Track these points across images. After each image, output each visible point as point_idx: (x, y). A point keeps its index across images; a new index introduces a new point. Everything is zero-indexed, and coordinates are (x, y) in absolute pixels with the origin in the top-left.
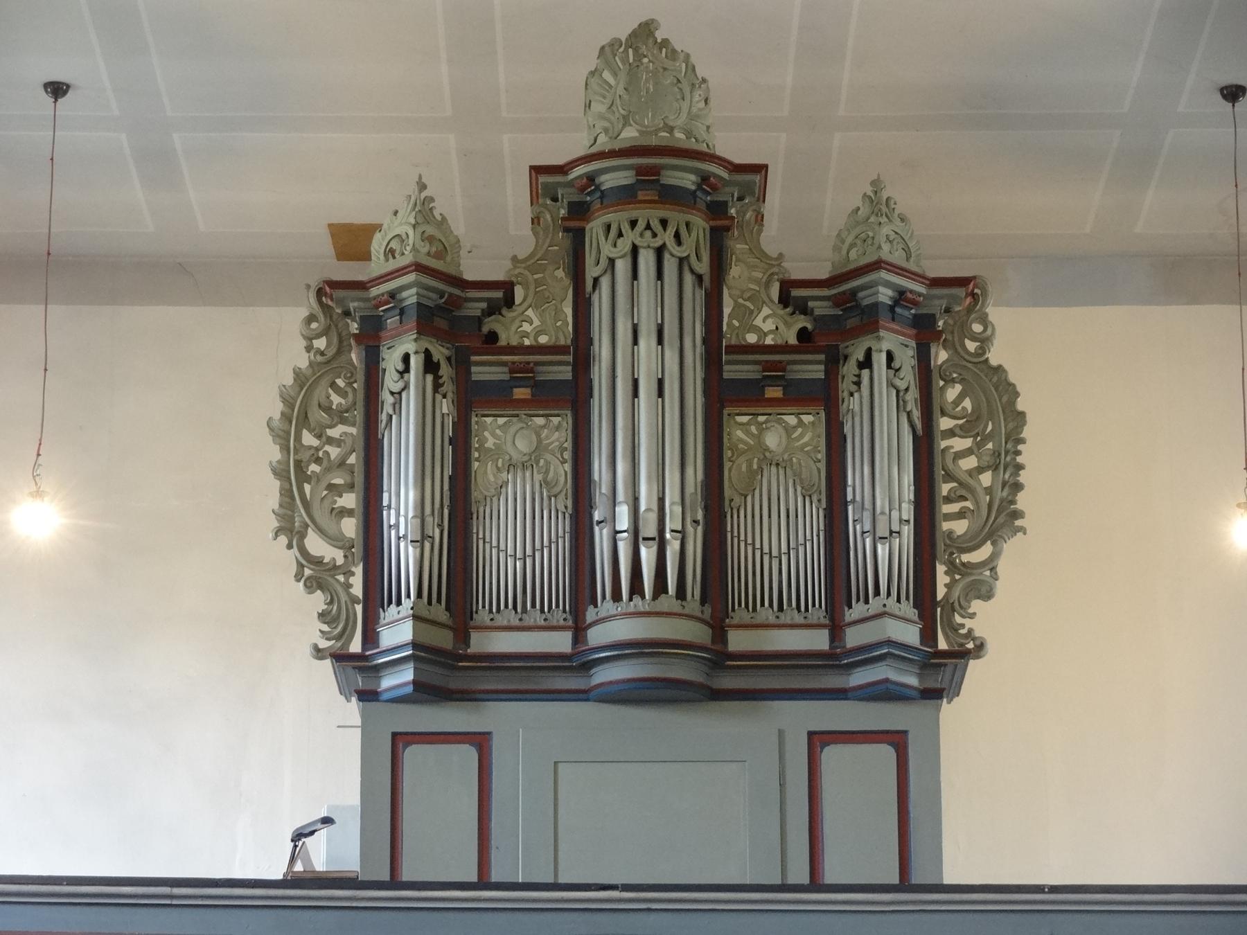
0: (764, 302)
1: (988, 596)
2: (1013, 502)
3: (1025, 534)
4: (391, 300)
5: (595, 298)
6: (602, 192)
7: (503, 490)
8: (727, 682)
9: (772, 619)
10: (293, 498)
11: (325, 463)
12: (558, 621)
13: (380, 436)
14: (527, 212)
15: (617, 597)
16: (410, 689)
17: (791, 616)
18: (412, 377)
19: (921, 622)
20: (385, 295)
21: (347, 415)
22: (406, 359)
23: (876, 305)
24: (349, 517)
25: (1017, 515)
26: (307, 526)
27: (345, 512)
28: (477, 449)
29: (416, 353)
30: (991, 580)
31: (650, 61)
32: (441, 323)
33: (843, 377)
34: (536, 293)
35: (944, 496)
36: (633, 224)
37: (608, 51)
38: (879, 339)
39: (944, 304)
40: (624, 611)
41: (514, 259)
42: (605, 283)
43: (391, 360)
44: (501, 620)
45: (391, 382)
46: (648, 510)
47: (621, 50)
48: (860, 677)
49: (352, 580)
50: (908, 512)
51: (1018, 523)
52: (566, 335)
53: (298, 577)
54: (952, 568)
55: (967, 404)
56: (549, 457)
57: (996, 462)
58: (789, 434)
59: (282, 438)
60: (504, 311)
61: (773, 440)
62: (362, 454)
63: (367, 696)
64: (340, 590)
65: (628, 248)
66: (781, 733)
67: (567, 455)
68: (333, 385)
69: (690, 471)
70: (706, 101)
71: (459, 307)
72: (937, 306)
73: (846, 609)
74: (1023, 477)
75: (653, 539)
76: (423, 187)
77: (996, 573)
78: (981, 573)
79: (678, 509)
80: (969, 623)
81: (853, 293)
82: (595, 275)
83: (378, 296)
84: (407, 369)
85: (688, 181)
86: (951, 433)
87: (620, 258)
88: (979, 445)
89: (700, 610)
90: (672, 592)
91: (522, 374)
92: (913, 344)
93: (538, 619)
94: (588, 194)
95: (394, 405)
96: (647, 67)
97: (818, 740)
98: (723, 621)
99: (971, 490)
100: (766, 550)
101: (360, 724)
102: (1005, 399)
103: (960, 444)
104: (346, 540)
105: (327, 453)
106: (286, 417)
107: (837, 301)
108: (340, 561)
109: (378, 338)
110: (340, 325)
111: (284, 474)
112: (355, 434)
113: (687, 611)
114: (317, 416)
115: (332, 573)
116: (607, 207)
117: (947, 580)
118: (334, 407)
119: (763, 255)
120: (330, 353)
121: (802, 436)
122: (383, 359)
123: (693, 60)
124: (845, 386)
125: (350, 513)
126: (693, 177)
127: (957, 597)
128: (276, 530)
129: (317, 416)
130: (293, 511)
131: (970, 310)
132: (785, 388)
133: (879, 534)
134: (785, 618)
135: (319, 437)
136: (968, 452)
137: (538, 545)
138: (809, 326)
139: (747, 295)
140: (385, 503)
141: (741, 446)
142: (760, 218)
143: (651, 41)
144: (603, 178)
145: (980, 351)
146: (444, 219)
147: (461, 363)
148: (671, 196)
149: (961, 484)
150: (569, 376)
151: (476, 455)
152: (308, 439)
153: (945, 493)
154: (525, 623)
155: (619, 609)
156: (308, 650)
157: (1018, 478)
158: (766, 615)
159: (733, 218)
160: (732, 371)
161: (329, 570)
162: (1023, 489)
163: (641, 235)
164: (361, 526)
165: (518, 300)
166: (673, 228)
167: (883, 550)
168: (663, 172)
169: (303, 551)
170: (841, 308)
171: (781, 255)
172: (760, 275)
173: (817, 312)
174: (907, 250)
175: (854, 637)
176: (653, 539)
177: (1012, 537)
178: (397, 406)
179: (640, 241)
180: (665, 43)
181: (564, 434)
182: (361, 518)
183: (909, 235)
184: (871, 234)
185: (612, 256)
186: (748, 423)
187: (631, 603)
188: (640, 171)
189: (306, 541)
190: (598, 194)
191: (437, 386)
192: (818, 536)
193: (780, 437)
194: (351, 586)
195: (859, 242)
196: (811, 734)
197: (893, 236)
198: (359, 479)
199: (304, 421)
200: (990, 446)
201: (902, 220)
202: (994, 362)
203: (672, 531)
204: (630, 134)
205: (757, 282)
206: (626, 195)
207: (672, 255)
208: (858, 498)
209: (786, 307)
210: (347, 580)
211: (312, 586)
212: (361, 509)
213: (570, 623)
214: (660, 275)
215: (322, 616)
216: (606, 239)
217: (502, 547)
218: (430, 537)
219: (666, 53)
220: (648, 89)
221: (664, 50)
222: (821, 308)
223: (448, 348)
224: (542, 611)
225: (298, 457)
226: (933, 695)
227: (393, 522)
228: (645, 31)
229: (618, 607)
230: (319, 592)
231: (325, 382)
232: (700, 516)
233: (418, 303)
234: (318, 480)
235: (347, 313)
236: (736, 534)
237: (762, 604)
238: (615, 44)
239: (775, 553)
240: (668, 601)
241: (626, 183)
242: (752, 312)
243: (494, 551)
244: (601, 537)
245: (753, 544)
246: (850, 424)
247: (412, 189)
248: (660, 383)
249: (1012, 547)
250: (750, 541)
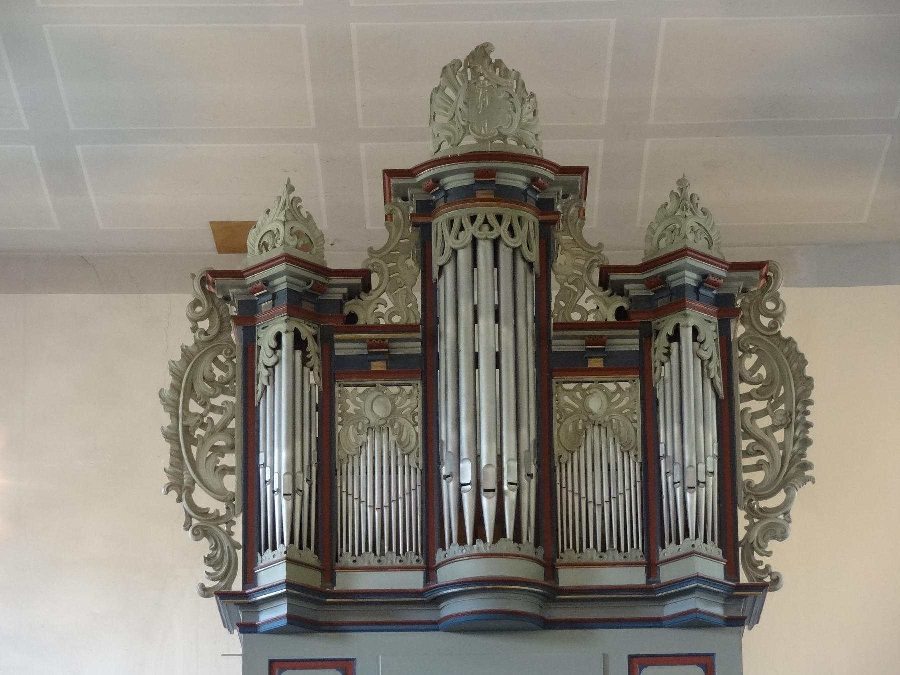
0: (586, 286)
1: (783, 537)
2: (803, 455)
3: (814, 483)
4: (265, 287)
5: (441, 283)
6: (446, 192)
7: (364, 450)
8: (559, 613)
9: (596, 559)
10: (182, 458)
11: (209, 428)
12: (412, 562)
13: (256, 404)
14: (382, 211)
15: (462, 541)
16: (284, 622)
17: (613, 556)
18: (284, 353)
19: (725, 560)
20: (260, 283)
21: (228, 386)
22: (278, 337)
23: (683, 288)
24: (231, 474)
25: (807, 466)
26: (194, 482)
27: (227, 470)
28: (340, 415)
29: (287, 332)
30: (785, 523)
31: (486, 79)
32: (307, 306)
33: (656, 349)
34: (390, 279)
35: (743, 451)
36: (473, 219)
37: (450, 71)
38: (686, 316)
39: (742, 285)
40: (468, 553)
41: (371, 251)
42: (449, 271)
43: (265, 339)
44: (362, 563)
45: (265, 357)
46: (488, 466)
47: (461, 70)
48: (673, 608)
49: (233, 529)
50: (713, 464)
51: (808, 473)
52: (416, 316)
53: (187, 526)
54: (752, 513)
55: (763, 371)
56: (402, 421)
57: (788, 421)
58: (609, 399)
59: (172, 406)
60: (363, 295)
61: (595, 404)
62: (241, 419)
63: (248, 629)
64: (223, 537)
65: (469, 239)
66: (605, 658)
67: (418, 419)
68: (216, 360)
69: (524, 432)
70: (535, 113)
71: (324, 292)
72: (735, 288)
73: (660, 549)
74: (812, 434)
75: (493, 491)
76: (291, 189)
77: (789, 517)
78: (777, 517)
79: (514, 465)
80: (766, 560)
81: (664, 277)
82: (441, 264)
83: (254, 284)
84: (279, 347)
85: (520, 182)
86: (749, 397)
87: (463, 248)
88: (774, 407)
89: (535, 552)
90: (510, 535)
91: (379, 350)
92: (716, 320)
93: (395, 561)
94: (434, 194)
95: (268, 377)
96: (484, 84)
98: (554, 561)
99: (767, 446)
100: (591, 499)
101: (241, 653)
102: (795, 366)
103: (757, 406)
104: (228, 494)
105: (210, 419)
106: (176, 389)
107: (650, 284)
108: (223, 512)
109: (254, 320)
110: (221, 309)
111: (174, 438)
112: (235, 402)
113: (523, 553)
114: (203, 387)
115: (216, 523)
116: (451, 205)
117: (747, 523)
118: (217, 379)
119: (585, 245)
120: (213, 333)
121: (620, 401)
122: (259, 338)
123: (524, 78)
124: (658, 357)
125: (231, 471)
126: (524, 179)
127: (756, 538)
128: (167, 486)
129: (203, 387)
131: (764, 290)
132: (605, 358)
133: (688, 484)
134: (608, 558)
135: (204, 405)
136: (764, 413)
137: (394, 498)
138: (626, 306)
139: (571, 280)
140: (262, 462)
141: (568, 410)
142: (582, 213)
143: (487, 61)
144: (447, 180)
145: (773, 326)
146: (310, 217)
147: (326, 340)
148: (506, 195)
149: (759, 441)
150: (419, 351)
151: (340, 419)
152: (195, 407)
153: (744, 448)
154: (384, 565)
155: (465, 551)
156: (196, 590)
157: (807, 435)
158: (591, 555)
159: (558, 213)
160: (559, 346)
161: (214, 520)
162: (812, 444)
163: (480, 229)
164: (241, 482)
165: (374, 286)
166: (507, 222)
167: (692, 498)
168: (498, 174)
169: (191, 504)
170: (654, 289)
171: (601, 245)
172: (582, 262)
173: (633, 294)
174: (710, 240)
175: (667, 574)
176: (493, 491)
177: (803, 486)
178: (271, 378)
179: (479, 234)
180: (499, 63)
181: (415, 401)
182: (241, 475)
183: (711, 226)
184: (678, 226)
185: (455, 247)
186: (574, 390)
187: (475, 546)
188: (479, 173)
189: (193, 495)
190: (443, 194)
191: (305, 361)
192: (636, 486)
193: (602, 401)
194: (232, 534)
195: (668, 233)
196: (631, 658)
197: (697, 228)
198: (239, 442)
199: (191, 391)
200: (783, 407)
201: (705, 214)
202: (785, 335)
203: (510, 484)
204: (469, 143)
205: (581, 269)
206: (467, 195)
207: (508, 246)
208: (670, 454)
209: (605, 289)
210: (229, 528)
211: (199, 535)
212: (241, 466)
213: (422, 564)
214: (496, 264)
215: (208, 560)
216: (450, 232)
217: (363, 499)
218: (301, 491)
219: (500, 73)
220: (484, 103)
221: (498, 70)
222: (635, 290)
223: (314, 328)
224: (398, 554)
225: (184, 424)
226: (736, 622)
227: (268, 478)
228: (482, 53)
229: (463, 550)
230: (205, 539)
231: (209, 357)
232: (533, 470)
233: (289, 290)
234: (203, 443)
235: (227, 299)
236: (564, 486)
237: (588, 546)
238: (456, 64)
239: (598, 501)
240: (507, 545)
241: (466, 184)
242: (576, 294)
243: (356, 503)
244: (449, 490)
245: (580, 494)
246: (662, 389)
247: (282, 191)
248: (498, 356)
249: (802, 494)
250: (576, 491)
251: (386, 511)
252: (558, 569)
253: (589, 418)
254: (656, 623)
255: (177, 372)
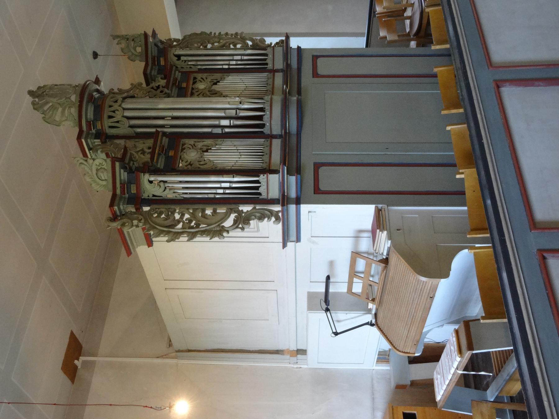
9: (271, 86)
11: (192, 219)
13: (183, 198)
27: (215, 211)
44: (267, 160)
48: (294, 65)
59: (177, 235)
97: (315, 74)
105: (186, 220)
106: (168, 233)
114: (168, 222)
130: (212, 231)
144: (88, 117)
173: (156, 73)
198: (201, 206)
213: (269, 140)
234: (199, 221)
238: (33, 103)
241: (93, 109)
254: (299, 69)
255: (158, 233)
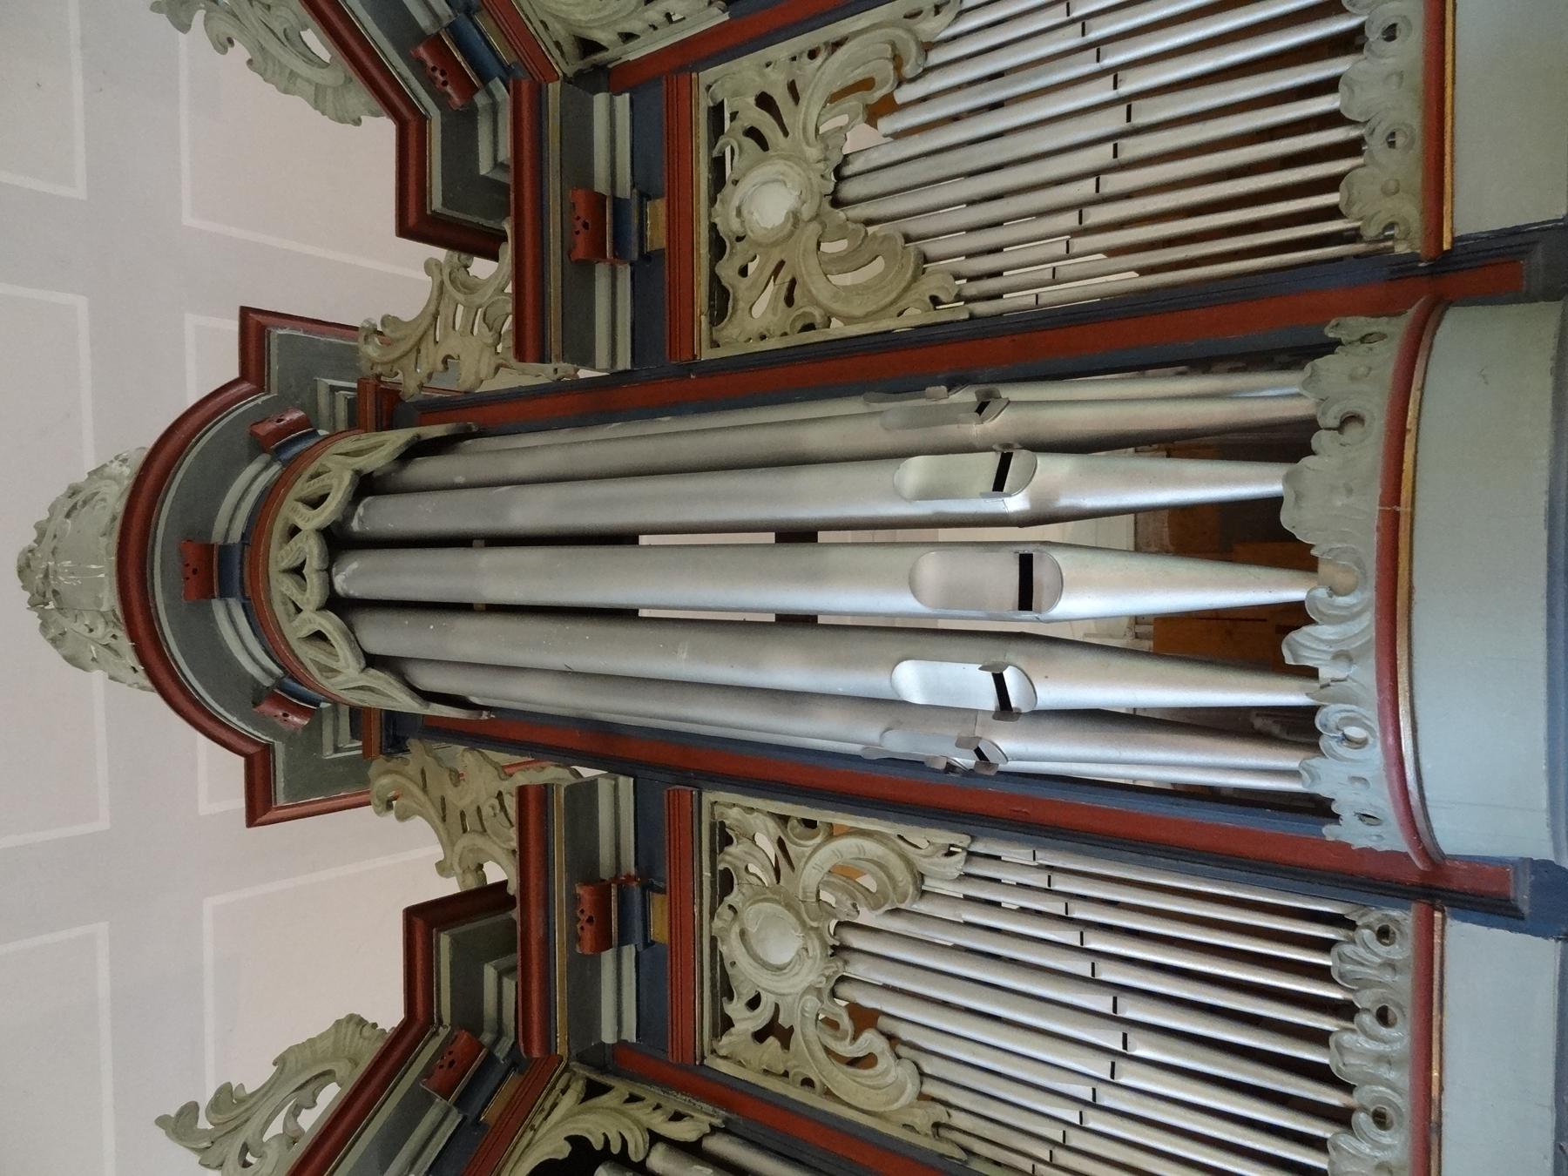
7: (905, 1033)
12: (1390, 965)
40: (1371, 714)
42: (431, 680)
90: (1272, 481)
93: (1381, 1047)
154: (1401, 1102)
155: (1354, 732)
187: (1325, 673)
193: (764, 183)
203: (999, 485)
213: (1404, 918)
229: (1346, 738)
239: (1114, 121)
243: (1095, 1121)
245: (1080, 206)
251: (1132, 1010)
252: (1454, 240)
253: (811, 220)
